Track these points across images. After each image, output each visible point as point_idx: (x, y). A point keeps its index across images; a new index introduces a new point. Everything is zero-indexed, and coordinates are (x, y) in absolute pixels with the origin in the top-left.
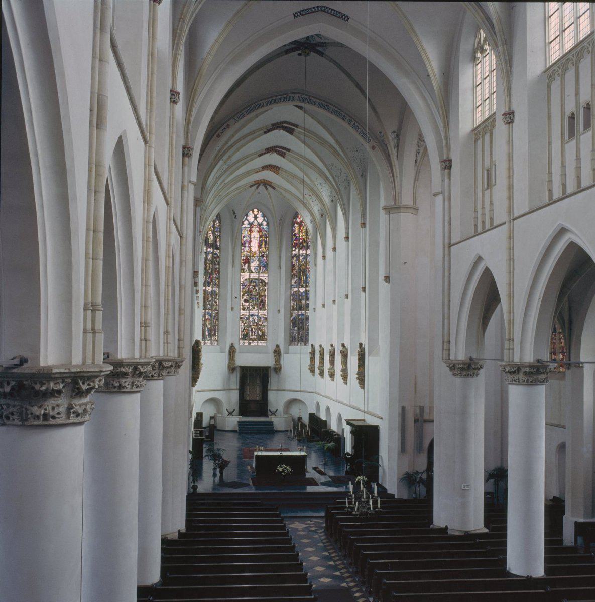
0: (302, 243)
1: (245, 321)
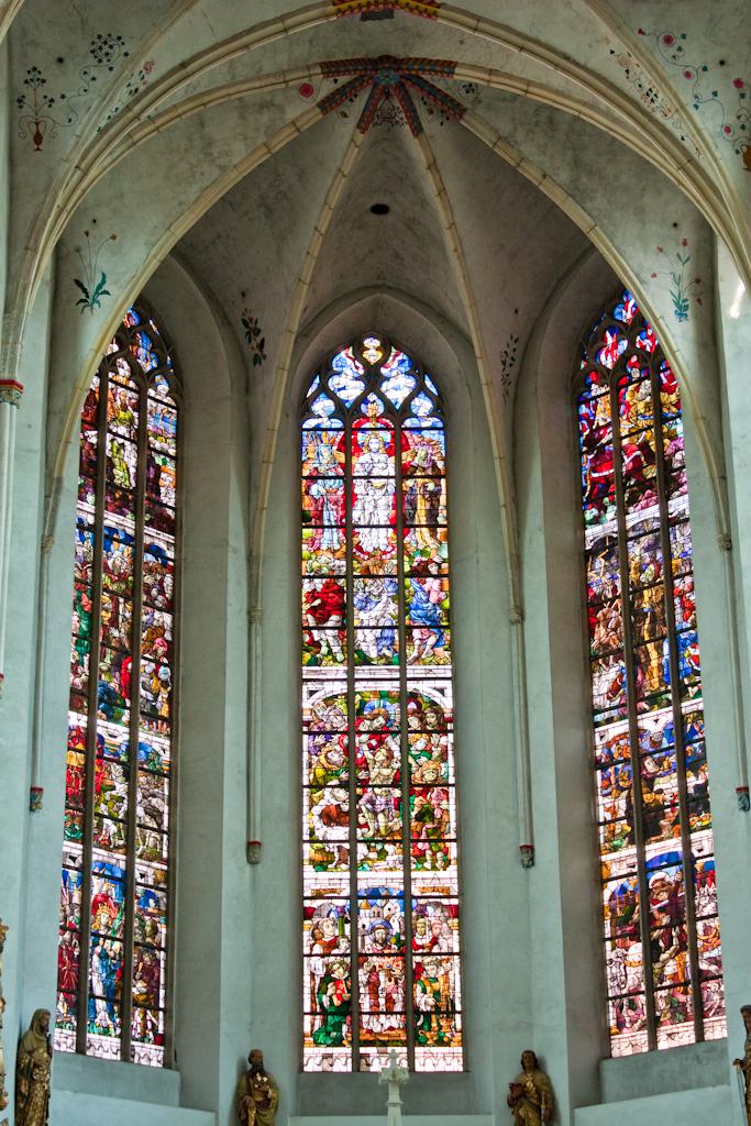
0: (637, 467)
1: (329, 932)
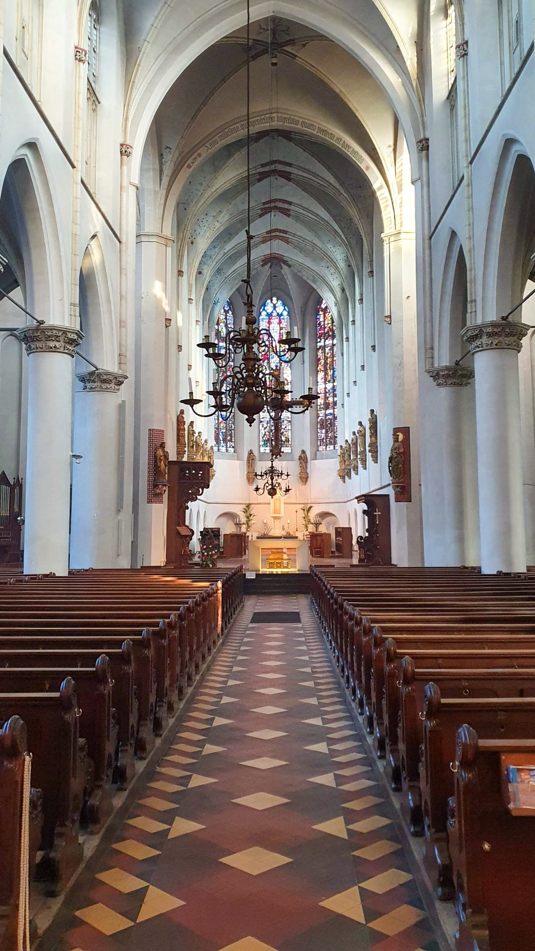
0: (328, 332)
